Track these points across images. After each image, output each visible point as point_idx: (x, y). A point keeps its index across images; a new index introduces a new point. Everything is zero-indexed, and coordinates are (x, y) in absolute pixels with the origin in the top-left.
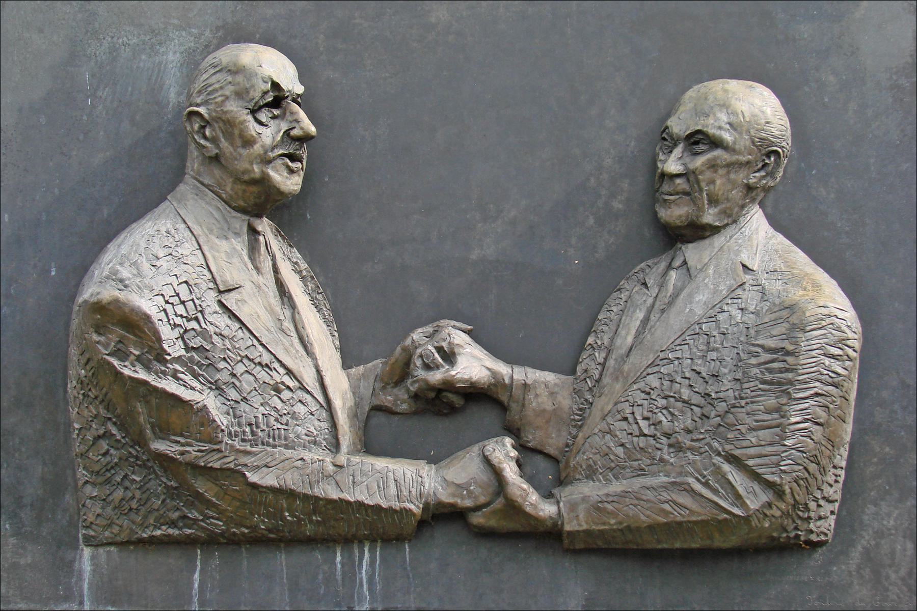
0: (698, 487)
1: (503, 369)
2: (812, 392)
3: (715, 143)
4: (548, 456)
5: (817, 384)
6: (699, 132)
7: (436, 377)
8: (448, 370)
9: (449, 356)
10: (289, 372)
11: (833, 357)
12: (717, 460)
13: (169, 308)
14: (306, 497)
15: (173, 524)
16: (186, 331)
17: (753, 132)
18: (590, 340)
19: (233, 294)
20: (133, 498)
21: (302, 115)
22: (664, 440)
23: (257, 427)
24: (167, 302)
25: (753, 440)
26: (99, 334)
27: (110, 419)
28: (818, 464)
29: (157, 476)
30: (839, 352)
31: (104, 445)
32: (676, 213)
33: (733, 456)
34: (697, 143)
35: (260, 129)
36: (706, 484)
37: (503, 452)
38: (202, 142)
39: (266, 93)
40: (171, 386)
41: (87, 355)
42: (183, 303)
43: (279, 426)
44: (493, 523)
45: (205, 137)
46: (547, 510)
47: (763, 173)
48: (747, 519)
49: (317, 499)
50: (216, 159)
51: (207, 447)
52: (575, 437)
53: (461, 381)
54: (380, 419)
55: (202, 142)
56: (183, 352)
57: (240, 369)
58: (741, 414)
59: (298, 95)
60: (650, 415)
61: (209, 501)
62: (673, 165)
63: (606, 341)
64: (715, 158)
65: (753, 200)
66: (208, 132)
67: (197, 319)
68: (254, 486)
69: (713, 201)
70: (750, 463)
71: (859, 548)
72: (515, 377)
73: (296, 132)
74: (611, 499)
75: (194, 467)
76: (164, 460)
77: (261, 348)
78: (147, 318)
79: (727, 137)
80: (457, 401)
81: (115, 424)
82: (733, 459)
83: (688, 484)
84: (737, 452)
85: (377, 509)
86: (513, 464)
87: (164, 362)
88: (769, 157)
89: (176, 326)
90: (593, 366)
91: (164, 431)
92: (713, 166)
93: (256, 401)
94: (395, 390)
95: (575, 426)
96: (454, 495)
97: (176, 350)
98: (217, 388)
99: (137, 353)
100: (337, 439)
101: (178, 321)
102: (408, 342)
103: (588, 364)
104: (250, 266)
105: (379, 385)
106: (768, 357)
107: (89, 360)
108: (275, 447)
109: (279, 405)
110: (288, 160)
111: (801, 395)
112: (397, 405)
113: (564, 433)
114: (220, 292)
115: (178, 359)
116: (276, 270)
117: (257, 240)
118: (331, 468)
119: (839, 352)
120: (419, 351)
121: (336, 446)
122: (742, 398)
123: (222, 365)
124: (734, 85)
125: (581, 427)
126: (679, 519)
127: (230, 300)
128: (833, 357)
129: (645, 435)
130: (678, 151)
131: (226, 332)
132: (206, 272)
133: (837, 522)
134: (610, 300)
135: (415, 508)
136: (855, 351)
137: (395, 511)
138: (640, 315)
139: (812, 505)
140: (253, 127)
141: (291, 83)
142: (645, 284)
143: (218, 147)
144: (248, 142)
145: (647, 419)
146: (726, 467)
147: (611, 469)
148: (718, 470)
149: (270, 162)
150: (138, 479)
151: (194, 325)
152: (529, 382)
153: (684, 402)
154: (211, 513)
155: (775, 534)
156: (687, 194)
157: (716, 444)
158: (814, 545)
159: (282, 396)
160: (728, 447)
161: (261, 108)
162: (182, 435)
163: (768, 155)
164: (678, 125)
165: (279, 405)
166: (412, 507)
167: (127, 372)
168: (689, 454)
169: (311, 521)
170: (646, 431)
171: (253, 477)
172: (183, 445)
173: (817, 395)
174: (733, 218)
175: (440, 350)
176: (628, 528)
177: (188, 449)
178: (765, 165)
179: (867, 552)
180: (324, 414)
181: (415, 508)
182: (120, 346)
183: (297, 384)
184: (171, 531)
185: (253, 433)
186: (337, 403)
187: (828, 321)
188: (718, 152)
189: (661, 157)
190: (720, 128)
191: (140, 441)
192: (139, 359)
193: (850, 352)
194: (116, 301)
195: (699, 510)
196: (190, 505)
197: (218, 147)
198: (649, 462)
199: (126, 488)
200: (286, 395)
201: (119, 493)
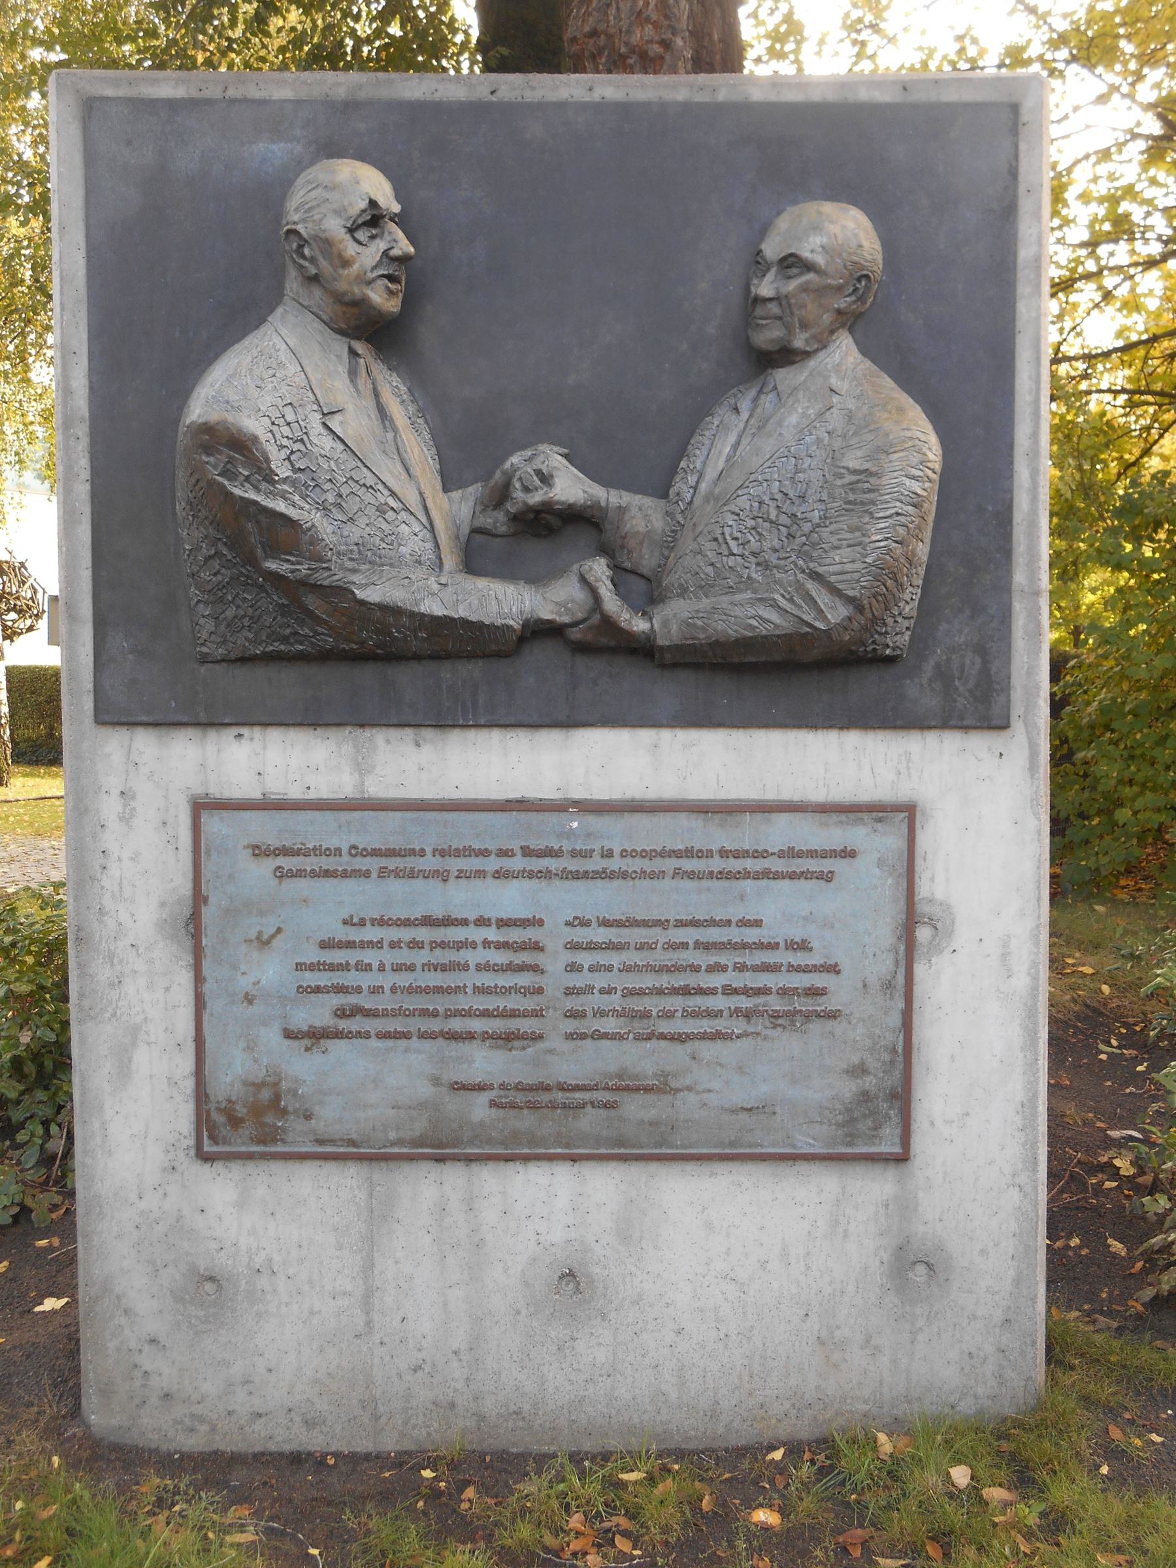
0: (783, 602)
1: (599, 493)
2: (893, 511)
4: (642, 576)
5: (898, 504)
6: (792, 255)
7: (535, 498)
8: (546, 493)
9: (546, 479)
10: (393, 494)
11: (913, 478)
12: (800, 576)
13: (275, 428)
15: (285, 640)
16: (292, 452)
17: (844, 255)
18: (683, 464)
19: (338, 417)
21: (400, 234)
22: (753, 560)
24: (273, 423)
25: (837, 558)
26: (208, 455)
27: (220, 539)
28: (896, 581)
29: (268, 593)
30: (920, 473)
31: (216, 564)
32: (768, 336)
33: (817, 573)
35: (360, 249)
36: (791, 600)
38: (302, 262)
39: (364, 211)
40: (280, 506)
41: (196, 476)
42: (289, 424)
43: (384, 545)
44: (589, 637)
45: (303, 257)
46: (640, 625)
47: (853, 298)
49: (423, 615)
50: (315, 279)
51: (315, 565)
52: (667, 558)
53: (557, 503)
54: (479, 538)
55: (302, 262)
56: (289, 473)
57: (345, 491)
58: (825, 533)
59: (396, 215)
60: (739, 535)
61: (319, 617)
62: (765, 288)
63: (698, 465)
64: (807, 282)
65: (843, 325)
66: (307, 251)
67: (302, 441)
68: (363, 603)
69: (804, 326)
70: (833, 579)
71: (932, 663)
72: (611, 500)
73: (396, 252)
74: (701, 615)
75: (303, 583)
76: (276, 578)
77: (365, 470)
78: (255, 439)
79: (820, 260)
80: (555, 522)
81: (225, 544)
82: (816, 576)
83: (774, 600)
84: (820, 570)
85: (479, 626)
86: (608, 583)
87: (272, 482)
88: (859, 280)
90: (686, 489)
91: (275, 549)
92: (805, 289)
93: (362, 521)
94: (495, 513)
95: (667, 548)
96: (552, 612)
97: (283, 471)
98: (324, 508)
99: (246, 473)
100: (440, 559)
101: (285, 442)
102: (507, 465)
103: (681, 487)
104: (353, 390)
105: (479, 508)
106: (854, 478)
107: (198, 481)
108: (382, 565)
109: (384, 526)
111: (881, 515)
112: (496, 528)
113: (656, 554)
114: (324, 414)
115: (285, 480)
116: (376, 394)
118: (435, 587)
119: (920, 473)
120: (518, 473)
122: (826, 518)
123: (327, 486)
124: (828, 207)
125: (673, 548)
126: (764, 632)
127: (334, 423)
128: (913, 478)
129: (734, 555)
130: (770, 276)
133: (912, 636)
134: (702, 425)
135: (516, 624)
137: (497, 627)
138: (732, 439)
139: (890, 621)
140: (351, 248)
141: (389, 202)
143: (317, 266)
144: (346, 263)
145: (736, 539)
147: (702, 588)
148: (799, 586)
149: (369, 283)
150: (249, 597)
151: (297, 446)
153: (772, 522)
154: (321, 630)
156: (780, 318)
157: (801, 562)
158: (891, 660)
159: (386, 516)
160: (812, 565)
161: (358, 227)
162: (291, 554)
163: (859, 280)
164: (772, 249)
165: (384, 526)
166: (511, 623)
167: (237, 492)
168: (775, 571)
169: (416, 637)
170: (735, 552)
171: (360, 594)
172: (293, 564)
173: (898, 514)
175: (539, 473)
176: (717, 641)
177: (298, 567)
178: (856, 289)
179: (938, 665)
180: (428, 535)
181: (516, 624)
182: (229, 466)
183: (401, 506)
184: (282, 647)
185: (360, 552)
186: (439, 524)
187: (910, 444)
188: (811, 276)
189: (755, 281)
191: (251, 560)
192: (247, 479)
194: (223, 422)
195: (784, 624)
196: (301, 623)
197: (317, 266)
198: (737, 580)
200: (390, 515)
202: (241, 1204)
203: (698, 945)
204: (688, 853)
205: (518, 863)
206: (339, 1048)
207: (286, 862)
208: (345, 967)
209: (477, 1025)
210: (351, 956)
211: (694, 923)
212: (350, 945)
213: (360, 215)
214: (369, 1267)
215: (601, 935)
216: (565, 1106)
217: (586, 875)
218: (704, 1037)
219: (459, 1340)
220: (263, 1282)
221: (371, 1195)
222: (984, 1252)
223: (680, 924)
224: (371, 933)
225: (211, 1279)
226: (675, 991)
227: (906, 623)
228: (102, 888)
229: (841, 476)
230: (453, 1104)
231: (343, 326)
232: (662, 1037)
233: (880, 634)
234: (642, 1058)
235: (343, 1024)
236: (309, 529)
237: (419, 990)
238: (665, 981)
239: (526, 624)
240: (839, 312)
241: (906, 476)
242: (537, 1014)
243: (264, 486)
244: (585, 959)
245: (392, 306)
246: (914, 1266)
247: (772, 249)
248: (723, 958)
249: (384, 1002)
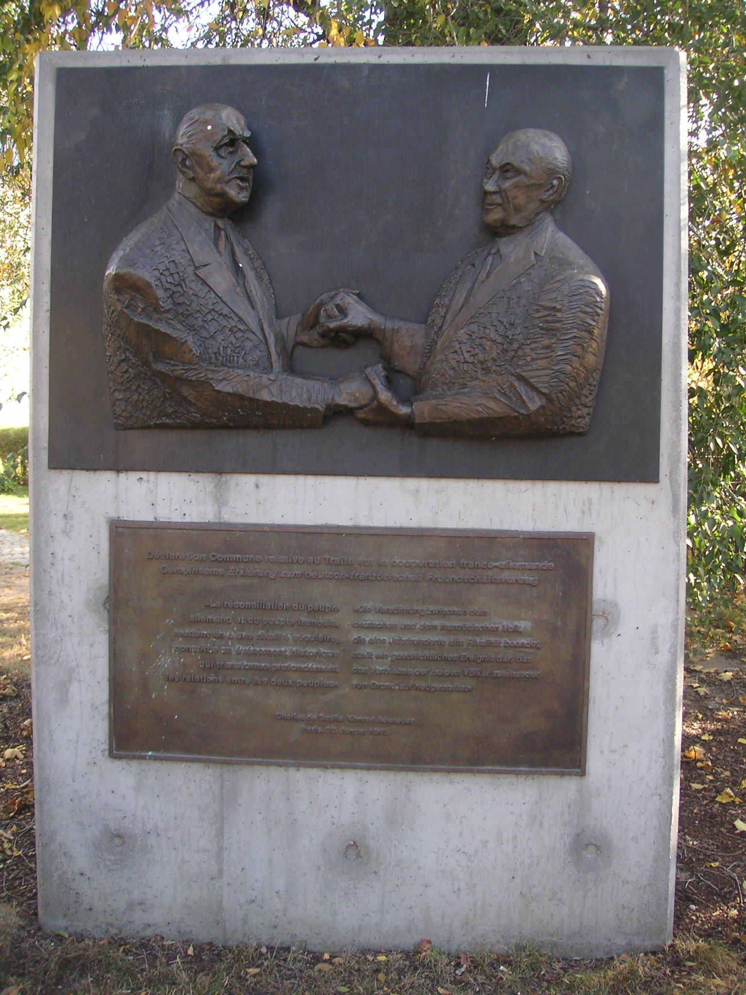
3: (518, 172)
6: (508, 164)
9: (343, 311)
10: (241, 319)
12: (513, 379)
13: (163, 278)
14: (251, 400)
15: (169, 416)
18: (437, 301)
20: (144, 400)
23: (220, 354)
28: (576, 382)
31: (124, 366)
32: (495, 216)
34: (507, 171)
37: (376, 373)
38: (184, 169)
39: (225, 137)
40: (163, 328)
41: (113, 308)
42: (172, 274)
44: (370, 417)
47: (551, 192)
48: (528, 416)
50: (193, 179)
53: (351, 326)
55: (184, 169)
59: (247, 138)
62: (490, 187)
68: (218, 392)
69: (517, 210)
75: (179, 379)
77: (223, 305)
79: (527, 168)
82: (521, 378)
89: (167, 290)
92: (516, 186)
93: (220, 338)
94: (311, 332)
97: (167, 305)
101: (168, 286)
104: (215, 251)
106: (546, 313)
110: (238, 181)
117: (220, 234)
121: (270, 369)
127: (202, 272)
130: (495, 177)
131: (199, 294)
132: (186, 254)
136: (602, 310)
139: (574, 409)
142: (473, 265)
144: (212, 170)
145: (469, 352)
146: (516, 384)
152: (396, 328)
155: (549, 427)
156: (500, 205)
158: (580, 434)
161: (221, 147)
162: (171, 359)
164: (496, 160)
172: (173, 365)
174: (530, 223)
181: (321, 408)
182: (132, 302)
183: (246, 328)
184: (167, 421)
185: (217, 359)
190: (522, 162)
191: (146, 363)
193: (599, 311)
197: (194, 172)
199: (140, 394)
200: (239, 335)
201: (135, 397)
202: (138, 789)
203: (443, 628)
213: (222, 140)
214: (220, 834)
219: (280, 884)
220: (152, 840)
221: (222, 787)
222: (635, 839)
225: (119, 836)
227: (586, 410)
228: (51, 577)
229: (538, 311)
231: (210, 209)
232: (418, 689)
233: (567, 418)
236: (183, 343)
239: (328, 407)
240: (542, 201)
241: (581, 311)
243: (155, 316)
245: (242, 197)
246: (588, 848)
247: (495, 161)
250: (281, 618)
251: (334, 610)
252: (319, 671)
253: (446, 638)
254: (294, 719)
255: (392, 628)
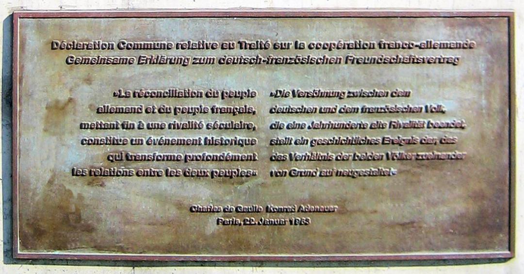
204: (357, 47)
205: (237, 53)
206: (112, 183)
207: (75, 54)
208: (114, 127)
209: (210, 167)
210: (120, 119)
211: (362, 95)
212: (120, 111)
215: (295, 103)
216: (272, 224)
217: (286, 62)
218: (371, 175)
223: (352, 95)
224: (134, 103)
226: (349, 143)
230: (192, 220)
234: (325, 189)
235: (115, 167)
237: (168, 143)
238: (343, 136)
242: (252, 159)
244: (285, 120)
248: (385, 120)
249: (144, 151)
250: (193, 103)
251: (251, 95)
252: (235, 159)
253: (367, 120)
254: (212, 211)
255: (313, 111)
